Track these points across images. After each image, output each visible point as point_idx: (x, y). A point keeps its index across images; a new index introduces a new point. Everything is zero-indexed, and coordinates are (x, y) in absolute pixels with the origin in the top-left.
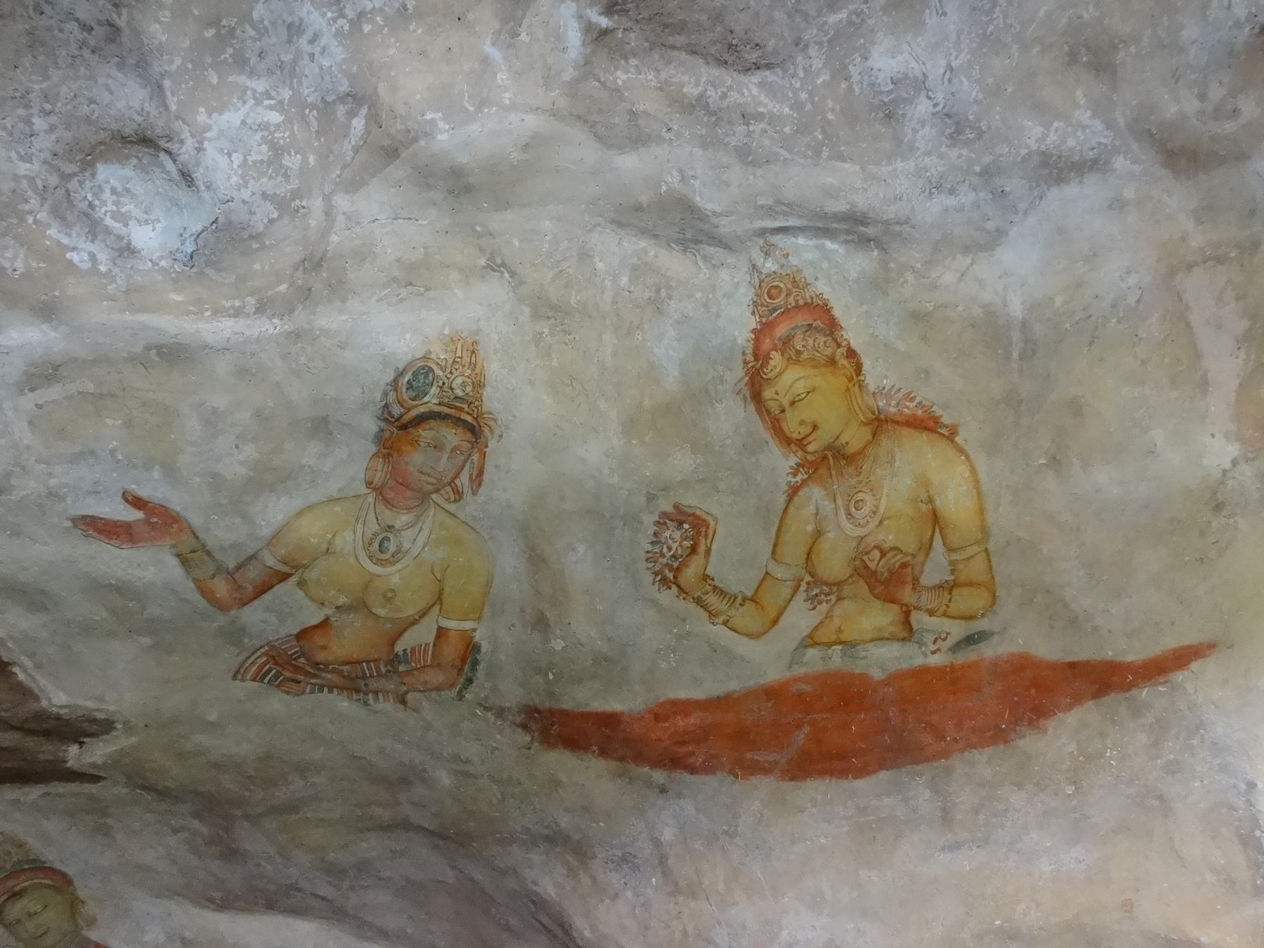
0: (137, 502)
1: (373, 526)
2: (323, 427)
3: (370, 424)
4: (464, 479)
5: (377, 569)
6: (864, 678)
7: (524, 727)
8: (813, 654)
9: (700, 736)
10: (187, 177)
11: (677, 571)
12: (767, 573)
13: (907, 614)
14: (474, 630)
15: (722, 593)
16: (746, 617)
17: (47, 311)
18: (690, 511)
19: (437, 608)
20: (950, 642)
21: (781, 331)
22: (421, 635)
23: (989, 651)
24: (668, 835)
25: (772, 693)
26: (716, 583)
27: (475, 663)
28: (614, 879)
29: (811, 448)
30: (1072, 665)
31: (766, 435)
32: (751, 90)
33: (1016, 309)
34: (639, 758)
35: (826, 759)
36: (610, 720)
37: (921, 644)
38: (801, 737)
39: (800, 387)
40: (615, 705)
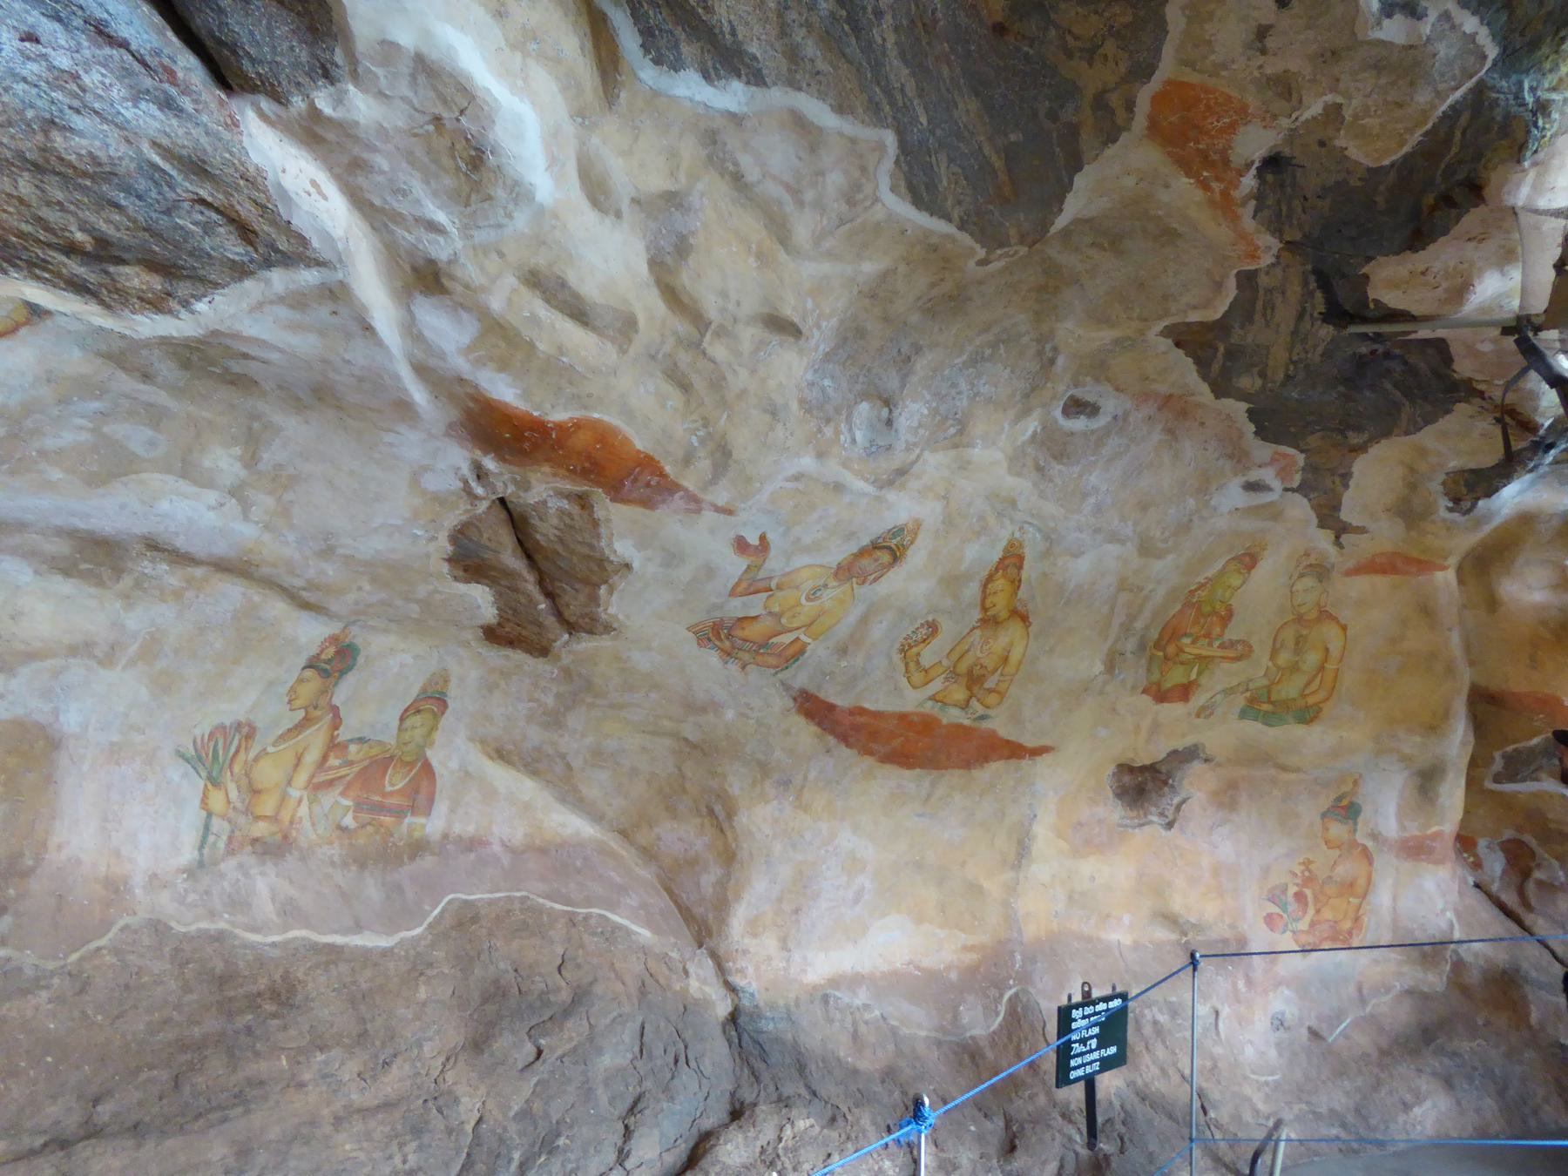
2: (850, 536)
3: (865, 541)
5: (803, 601)
7: (795, 699)
8: (930, 703)
9: (856, 728)
10: (889, 422)
11: (911, 647)
15: (918, 663)
16: (918, 678)
17: (821, 455)
22: (786, 639)
23: (986, 725)
24: (812, 775)
25: (903, 717)
28: (772, 792)
30: (1008, 742)
32: (1056, 468)
33: (1072, 585)
34: (832, 732)
35: (902, 758)
36: (831, 707)
38: (897, 743)
40: (838, 702)
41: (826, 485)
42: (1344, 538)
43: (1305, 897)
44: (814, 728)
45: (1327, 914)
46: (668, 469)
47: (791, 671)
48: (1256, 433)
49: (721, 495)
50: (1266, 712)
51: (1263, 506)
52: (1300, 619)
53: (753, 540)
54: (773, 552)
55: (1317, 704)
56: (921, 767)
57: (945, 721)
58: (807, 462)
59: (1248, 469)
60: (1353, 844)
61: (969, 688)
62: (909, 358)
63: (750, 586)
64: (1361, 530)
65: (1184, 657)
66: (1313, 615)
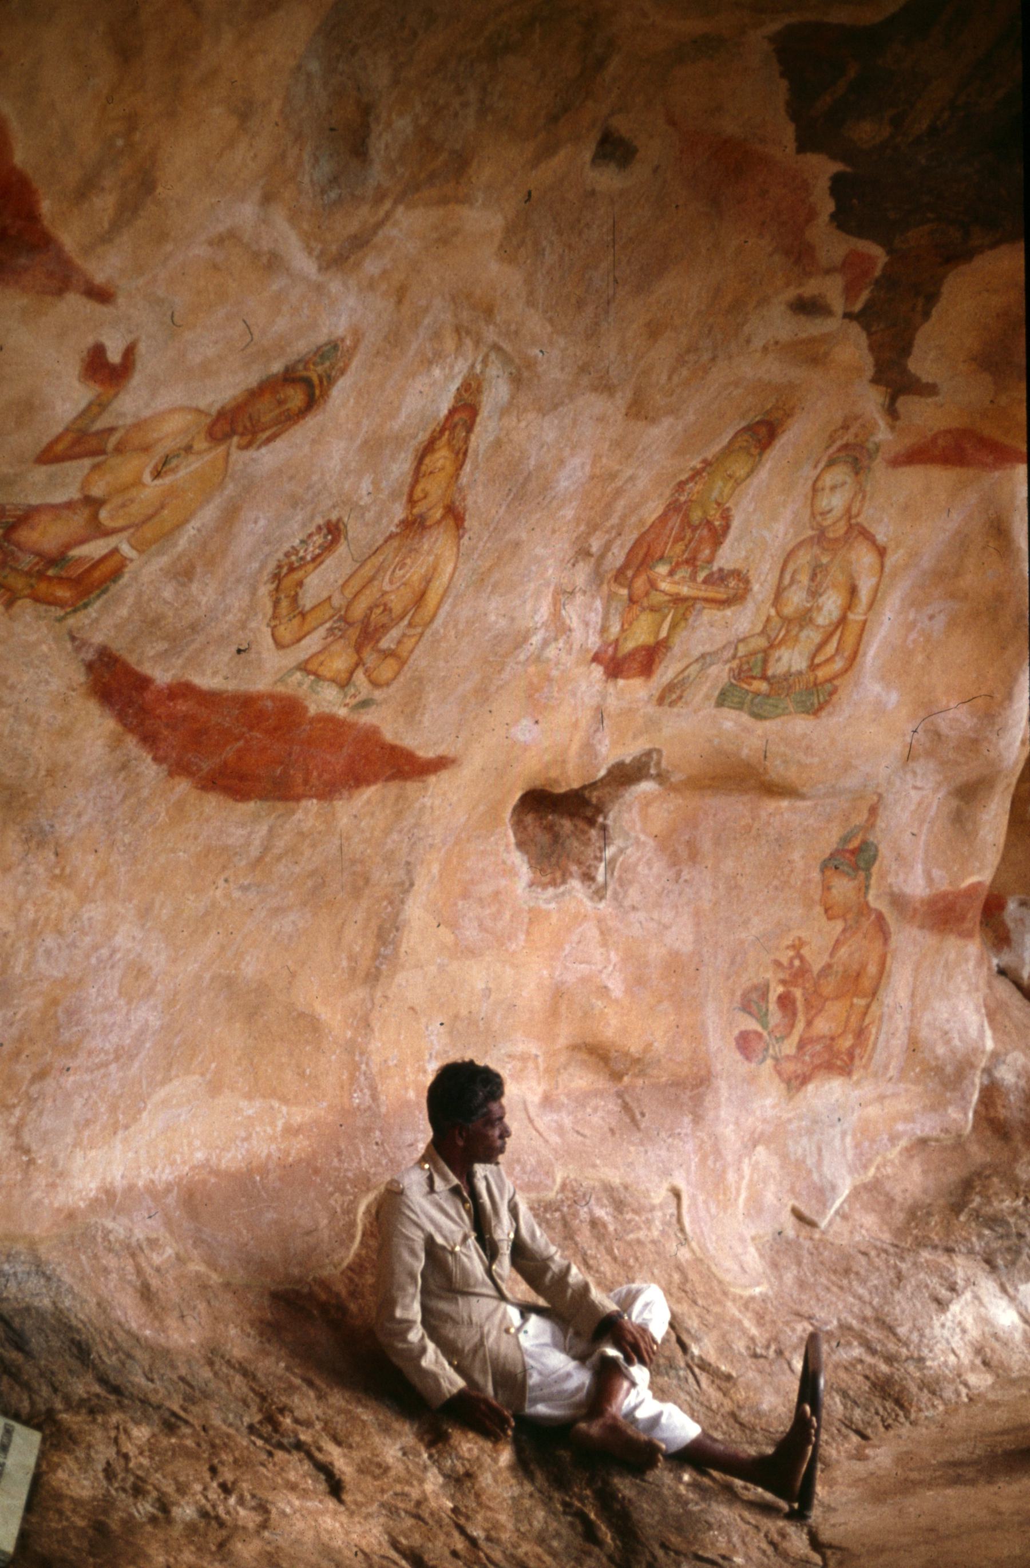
0: (129, 353)
1: (183, 444)
3: (277, 367)
4: (268, 433)
5: (147, 478)
6: (306, 709)
7: (90, 667)
8: (298, 675)
11: (292, 569)
12: (330, 598)
13: (357, 665)
14: (131, 560)
15: (295, 599)
18: (341, 526)
19: (132, 530)
20: (359, 698)
21: (456, 418)
23: (367, 718)
25: (246, 702)
26: (300, 592)
27: (104, 592)
29: (415, 511)
30: (393, 748)
31: (406, 489)
36: (144, 682)
37: (345, 696)
39: (439, 464)
41: (257, 255)
42: (903, 403)
43: (793, 1002)
44: (110, 724)
45: (822, 1026)
46: (46, 206)
47: (92, 611)
48: (833, 217)
49: (102, 269)
50: (757, 694)
51: (812, 340)
52: (821, 538)
53: (114, 357)
54: (136, 380)
55: (830, 680)
56: (263, 797)
57: (313, 710)
58: (247, 212)
59: (809, 275)
60: (864, 909)
61: (358, 649)
62: (415, 34)
63: (83, 442)
64: (931, 390)
65: (656, 598)
66: (841, 529)
